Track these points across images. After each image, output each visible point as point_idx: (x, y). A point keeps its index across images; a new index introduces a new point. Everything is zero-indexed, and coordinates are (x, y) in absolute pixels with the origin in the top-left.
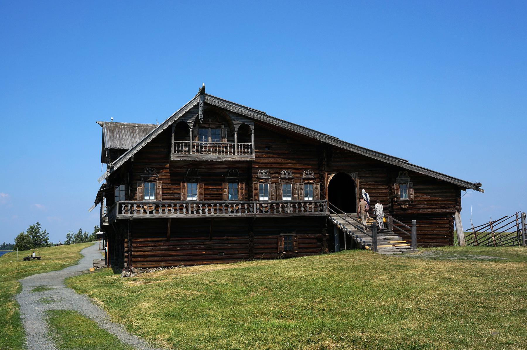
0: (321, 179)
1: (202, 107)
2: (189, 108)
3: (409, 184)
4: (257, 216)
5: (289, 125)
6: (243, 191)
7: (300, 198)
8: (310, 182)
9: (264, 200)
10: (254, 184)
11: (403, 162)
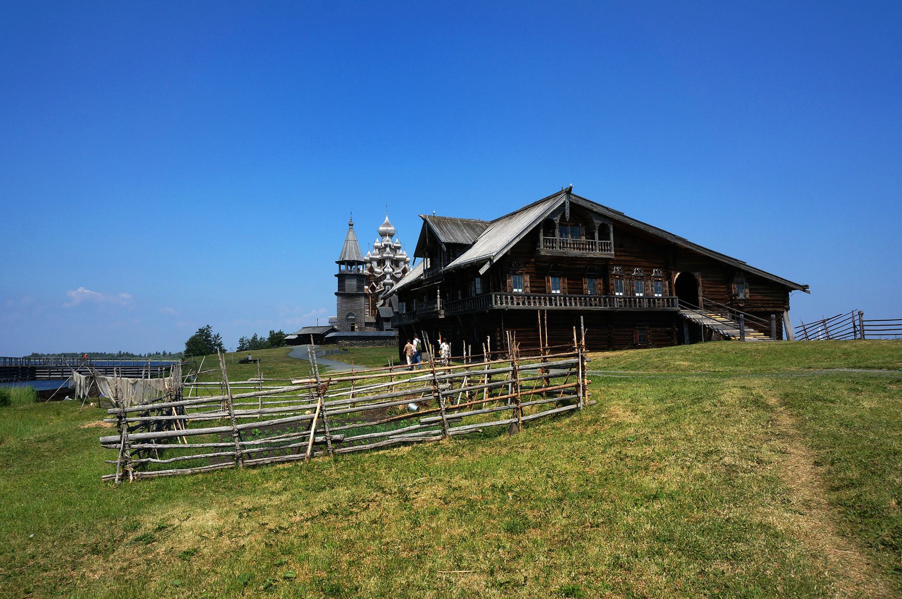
0: (669, 277)
7: (651, 294)
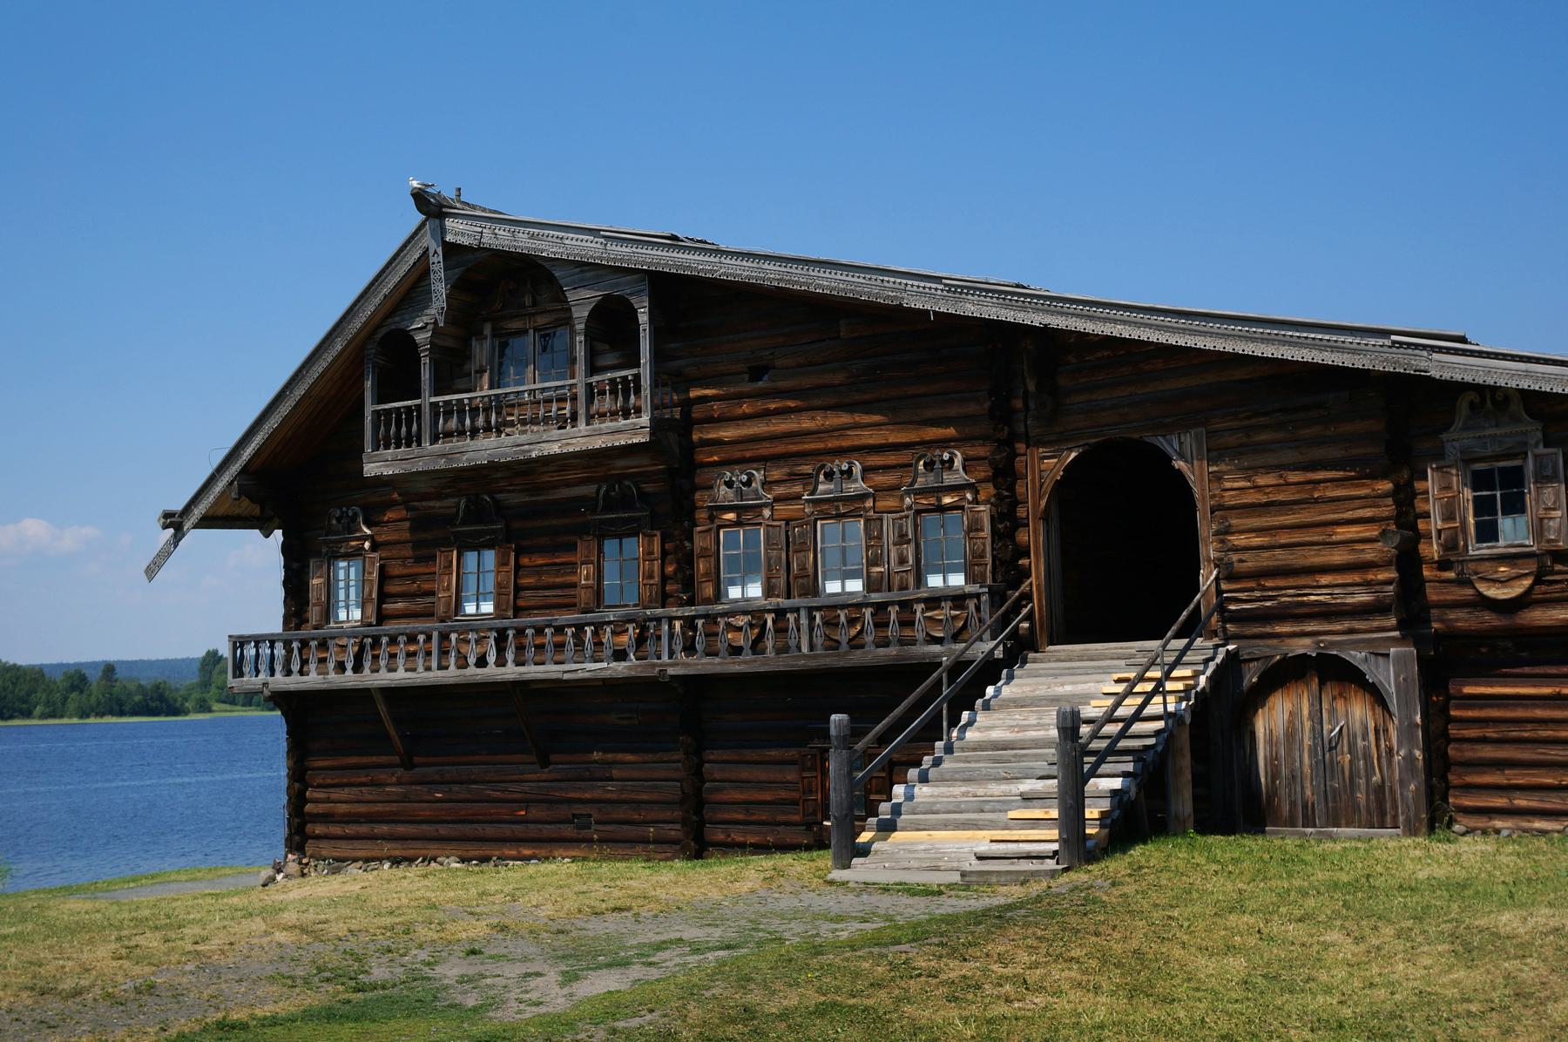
1: (437, 261)
2: (397, 279)
3: (1536, 456)
4: (671, 671)
5: (777, 268)
6: (653, 565)
8: (947, 500)
9: (844, 593)
10: (700, 532)
11: (1424, 347)
